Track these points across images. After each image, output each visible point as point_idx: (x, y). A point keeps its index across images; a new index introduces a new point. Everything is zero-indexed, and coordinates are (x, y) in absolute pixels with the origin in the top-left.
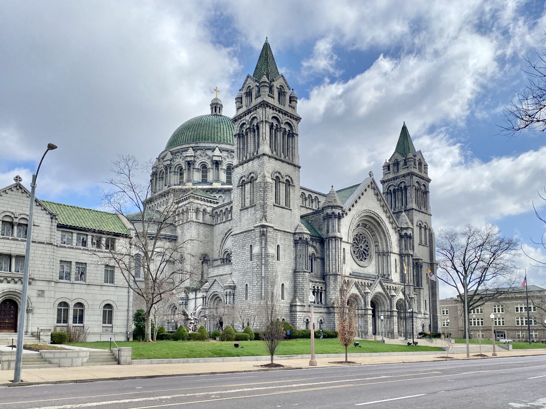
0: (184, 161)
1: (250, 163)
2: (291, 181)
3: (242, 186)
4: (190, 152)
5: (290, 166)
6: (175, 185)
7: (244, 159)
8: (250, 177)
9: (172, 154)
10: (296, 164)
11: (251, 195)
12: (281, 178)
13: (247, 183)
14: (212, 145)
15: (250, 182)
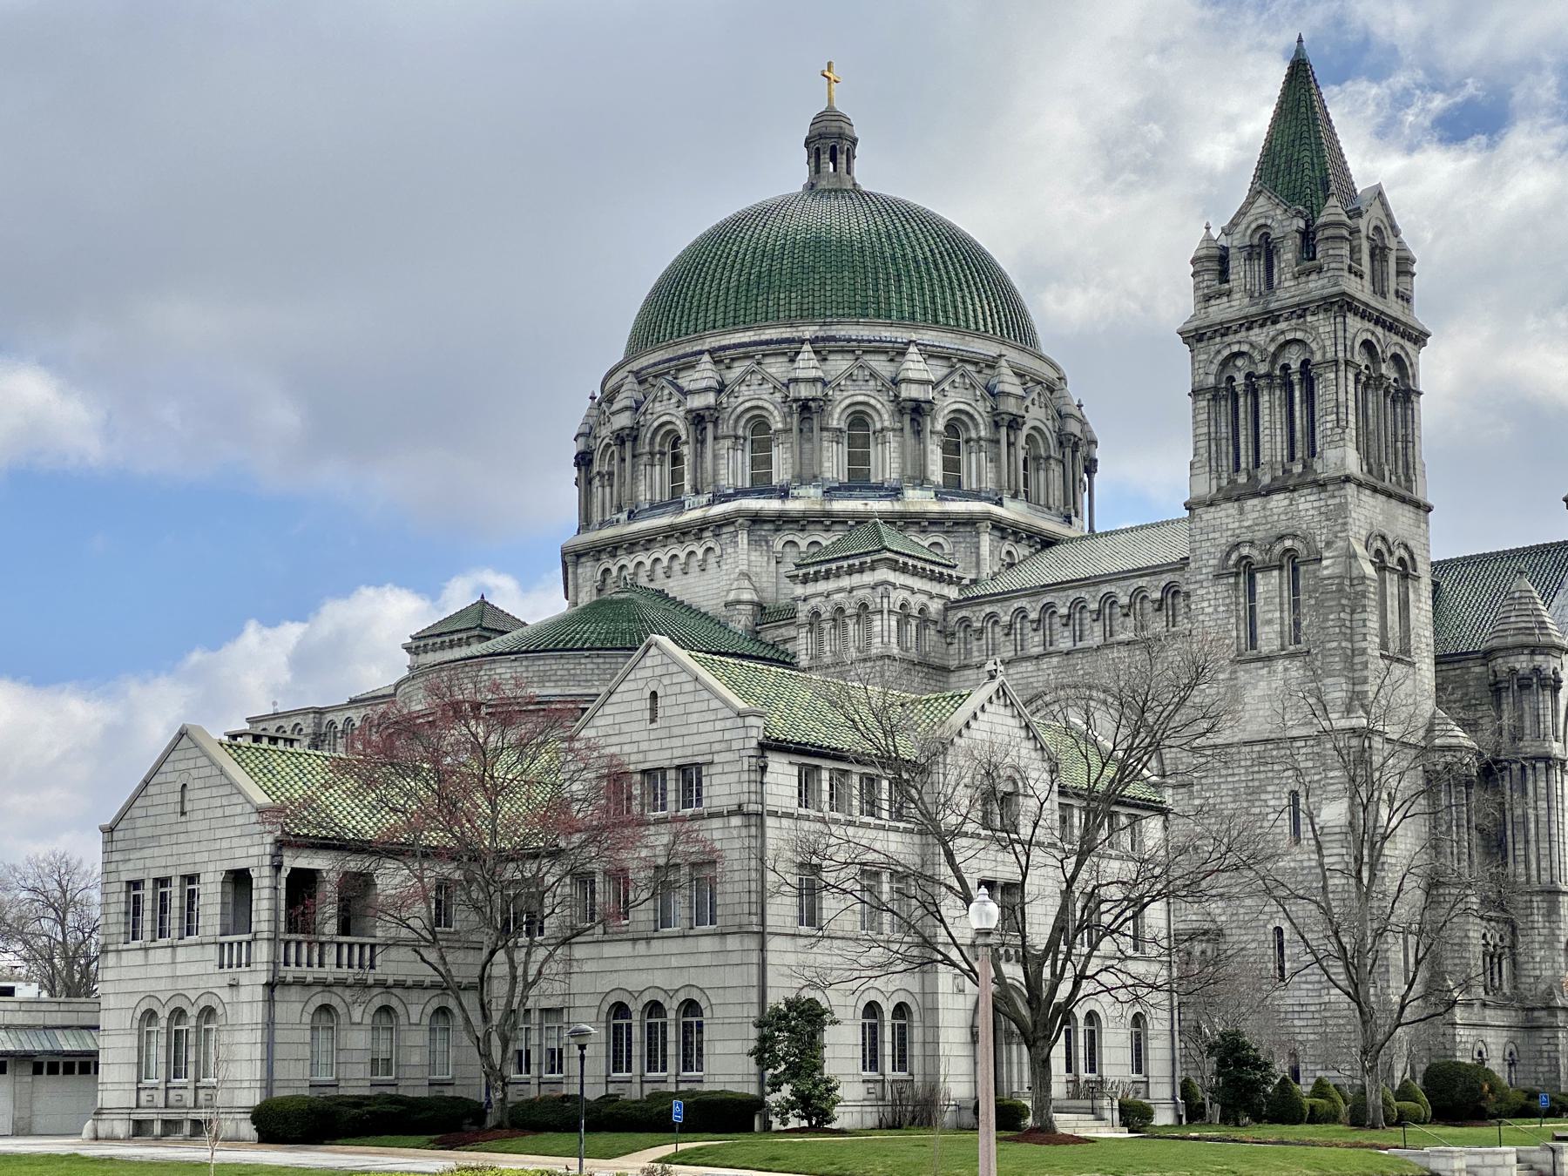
0: (778, 397)
1: (1279, 501)
2: (1409, 563)
3: (1237, 575)
4: (807, 365)
5: (1407, 507)
6: (740, 493)
7: (1242, 479)
8: (1278, 548)
9: (716, 363)
10: (1419, 495)
11: (1282, 611)
12: (1386, 555)
13: (1267, 568)
14: (886, 333)
15: (1281, 568)
